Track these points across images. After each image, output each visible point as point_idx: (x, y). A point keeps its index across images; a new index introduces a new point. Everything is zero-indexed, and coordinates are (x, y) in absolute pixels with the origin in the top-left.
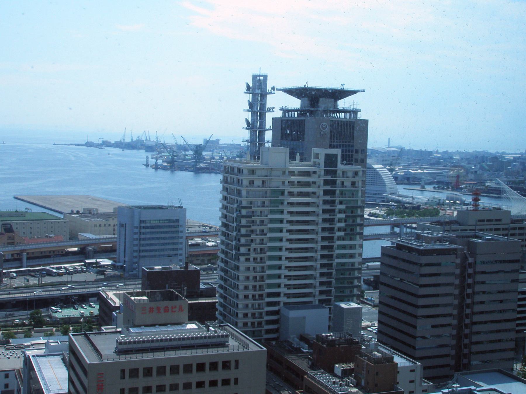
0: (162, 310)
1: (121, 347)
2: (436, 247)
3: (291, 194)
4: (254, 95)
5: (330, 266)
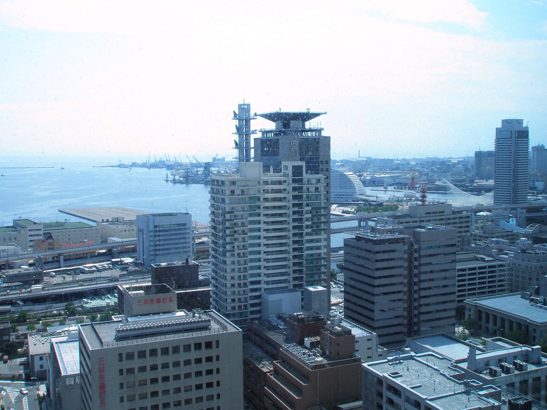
0: (155, 301)
1: (119, 334)
2: (387, 237)
3: (266, 200)
4: (240, 120)
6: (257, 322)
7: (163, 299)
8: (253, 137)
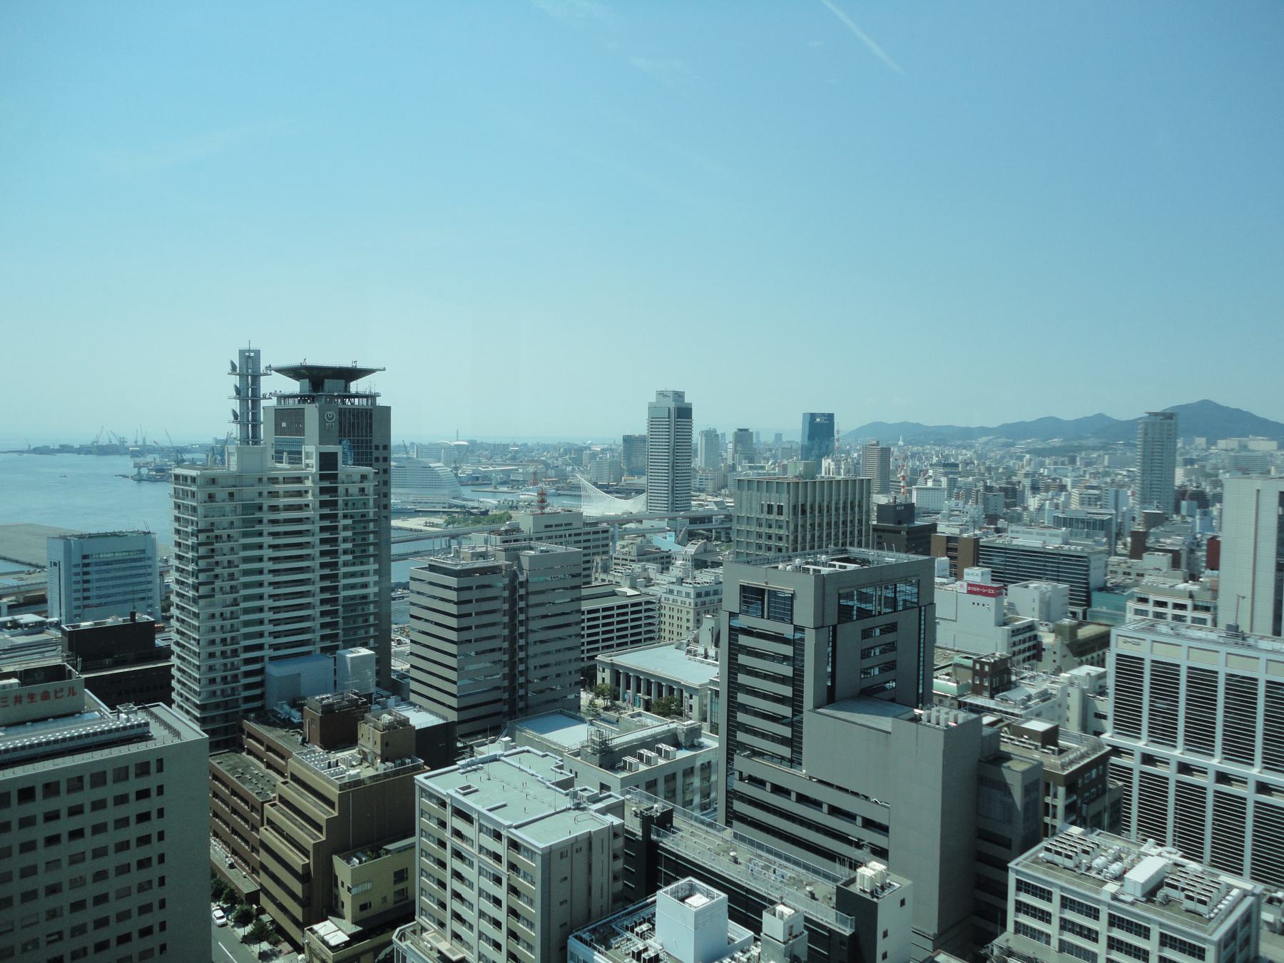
0: (38, 698)
3: (274, 508)
5: (334, 601)
7: (56, 692)
8: (264, 403)
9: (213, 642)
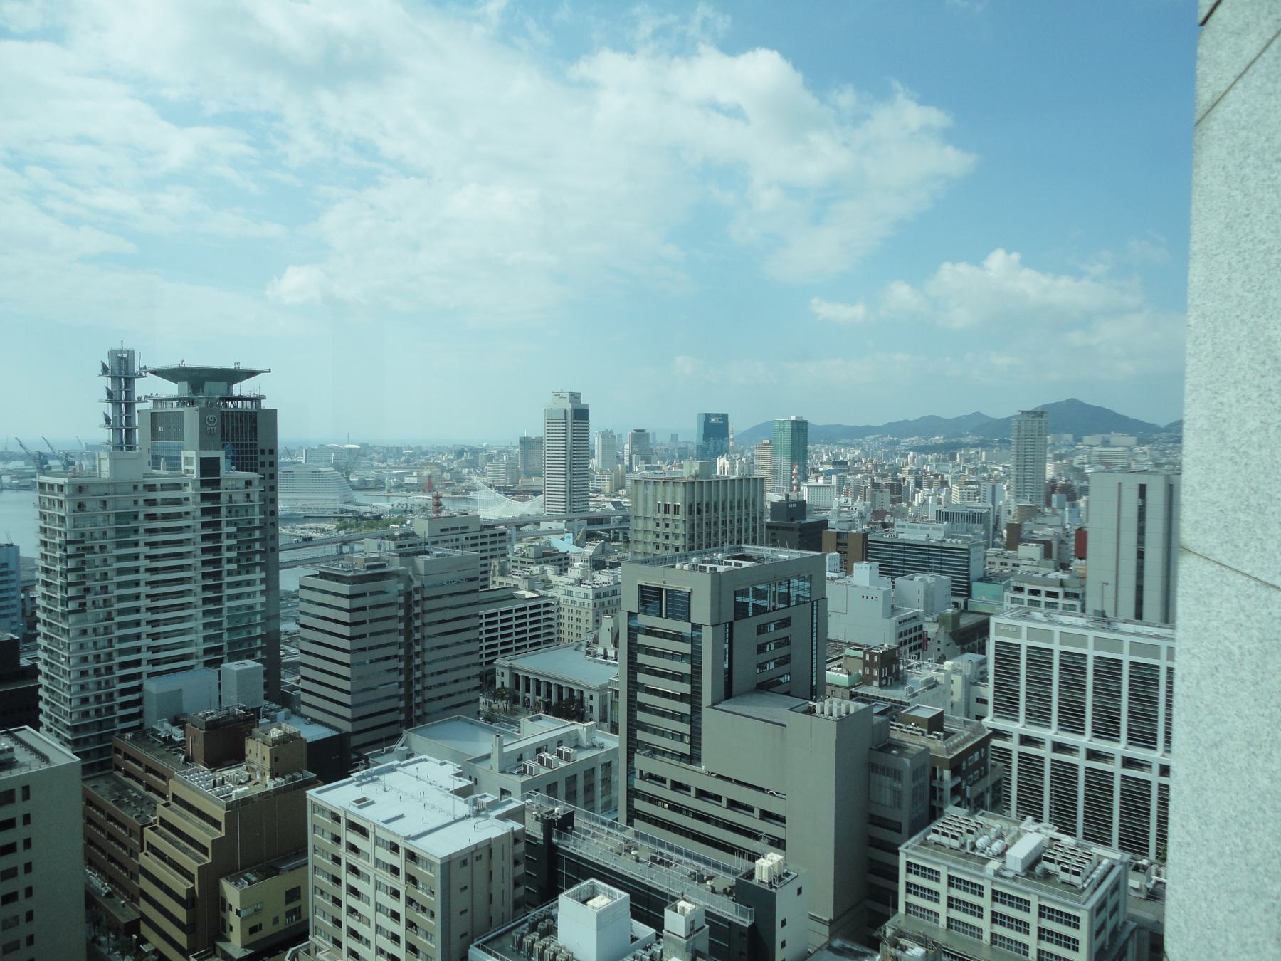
6: (129, 735)
8: (138, 406)
9: (85, 659)
